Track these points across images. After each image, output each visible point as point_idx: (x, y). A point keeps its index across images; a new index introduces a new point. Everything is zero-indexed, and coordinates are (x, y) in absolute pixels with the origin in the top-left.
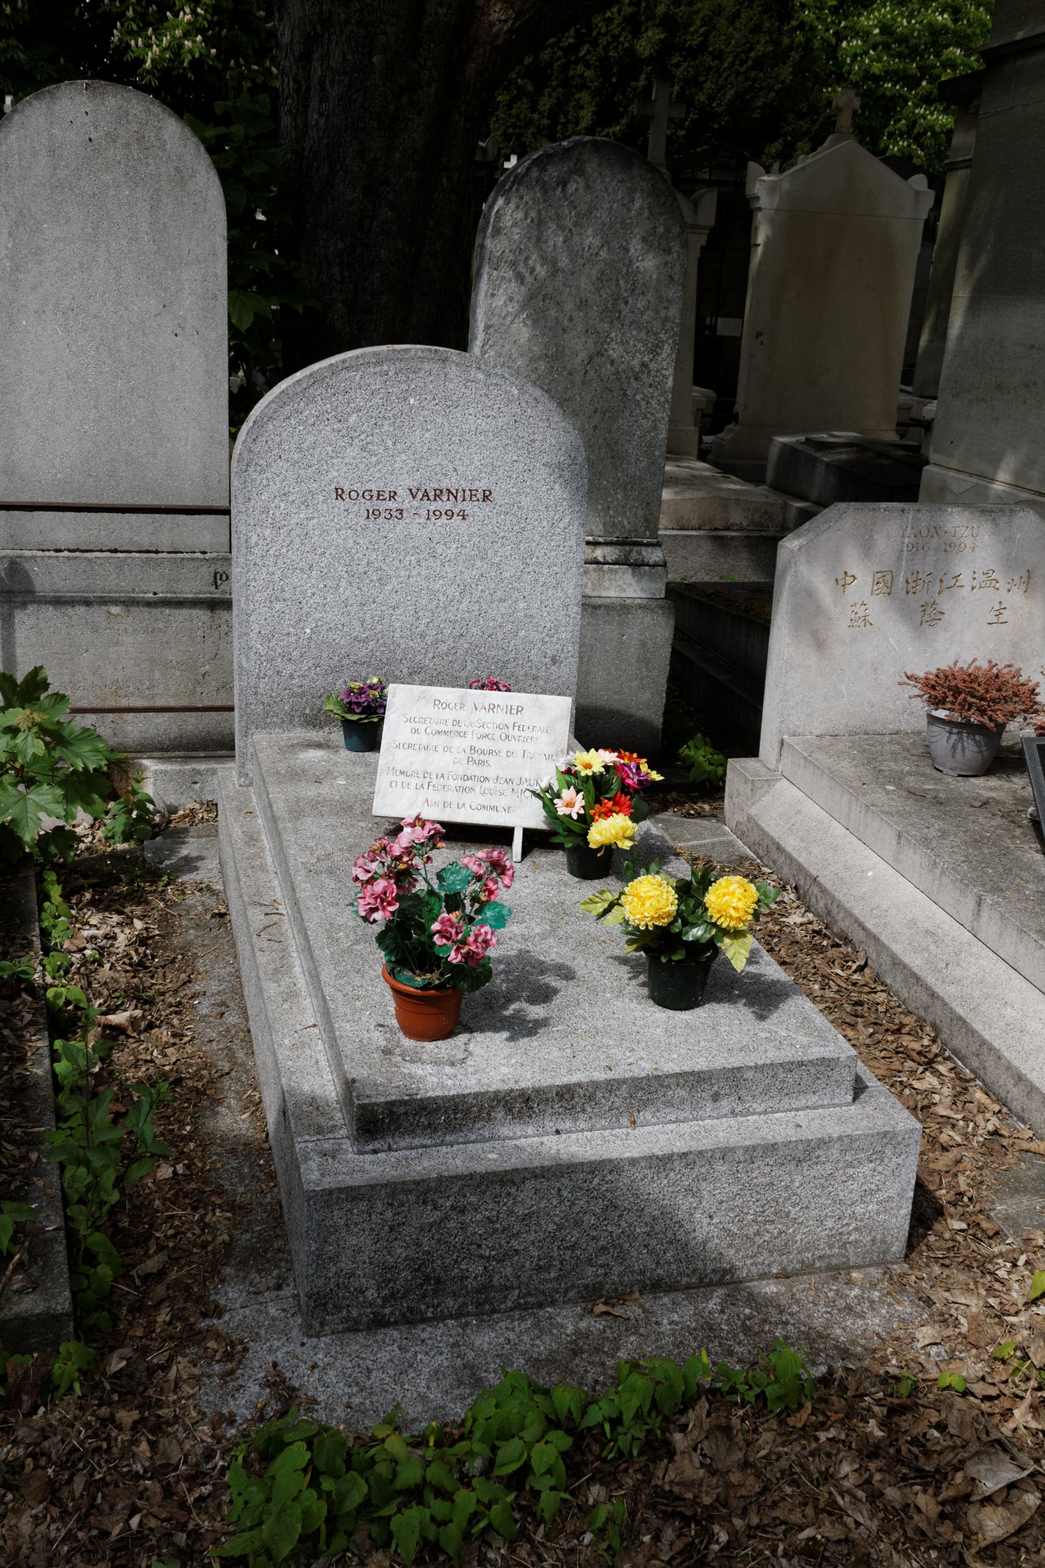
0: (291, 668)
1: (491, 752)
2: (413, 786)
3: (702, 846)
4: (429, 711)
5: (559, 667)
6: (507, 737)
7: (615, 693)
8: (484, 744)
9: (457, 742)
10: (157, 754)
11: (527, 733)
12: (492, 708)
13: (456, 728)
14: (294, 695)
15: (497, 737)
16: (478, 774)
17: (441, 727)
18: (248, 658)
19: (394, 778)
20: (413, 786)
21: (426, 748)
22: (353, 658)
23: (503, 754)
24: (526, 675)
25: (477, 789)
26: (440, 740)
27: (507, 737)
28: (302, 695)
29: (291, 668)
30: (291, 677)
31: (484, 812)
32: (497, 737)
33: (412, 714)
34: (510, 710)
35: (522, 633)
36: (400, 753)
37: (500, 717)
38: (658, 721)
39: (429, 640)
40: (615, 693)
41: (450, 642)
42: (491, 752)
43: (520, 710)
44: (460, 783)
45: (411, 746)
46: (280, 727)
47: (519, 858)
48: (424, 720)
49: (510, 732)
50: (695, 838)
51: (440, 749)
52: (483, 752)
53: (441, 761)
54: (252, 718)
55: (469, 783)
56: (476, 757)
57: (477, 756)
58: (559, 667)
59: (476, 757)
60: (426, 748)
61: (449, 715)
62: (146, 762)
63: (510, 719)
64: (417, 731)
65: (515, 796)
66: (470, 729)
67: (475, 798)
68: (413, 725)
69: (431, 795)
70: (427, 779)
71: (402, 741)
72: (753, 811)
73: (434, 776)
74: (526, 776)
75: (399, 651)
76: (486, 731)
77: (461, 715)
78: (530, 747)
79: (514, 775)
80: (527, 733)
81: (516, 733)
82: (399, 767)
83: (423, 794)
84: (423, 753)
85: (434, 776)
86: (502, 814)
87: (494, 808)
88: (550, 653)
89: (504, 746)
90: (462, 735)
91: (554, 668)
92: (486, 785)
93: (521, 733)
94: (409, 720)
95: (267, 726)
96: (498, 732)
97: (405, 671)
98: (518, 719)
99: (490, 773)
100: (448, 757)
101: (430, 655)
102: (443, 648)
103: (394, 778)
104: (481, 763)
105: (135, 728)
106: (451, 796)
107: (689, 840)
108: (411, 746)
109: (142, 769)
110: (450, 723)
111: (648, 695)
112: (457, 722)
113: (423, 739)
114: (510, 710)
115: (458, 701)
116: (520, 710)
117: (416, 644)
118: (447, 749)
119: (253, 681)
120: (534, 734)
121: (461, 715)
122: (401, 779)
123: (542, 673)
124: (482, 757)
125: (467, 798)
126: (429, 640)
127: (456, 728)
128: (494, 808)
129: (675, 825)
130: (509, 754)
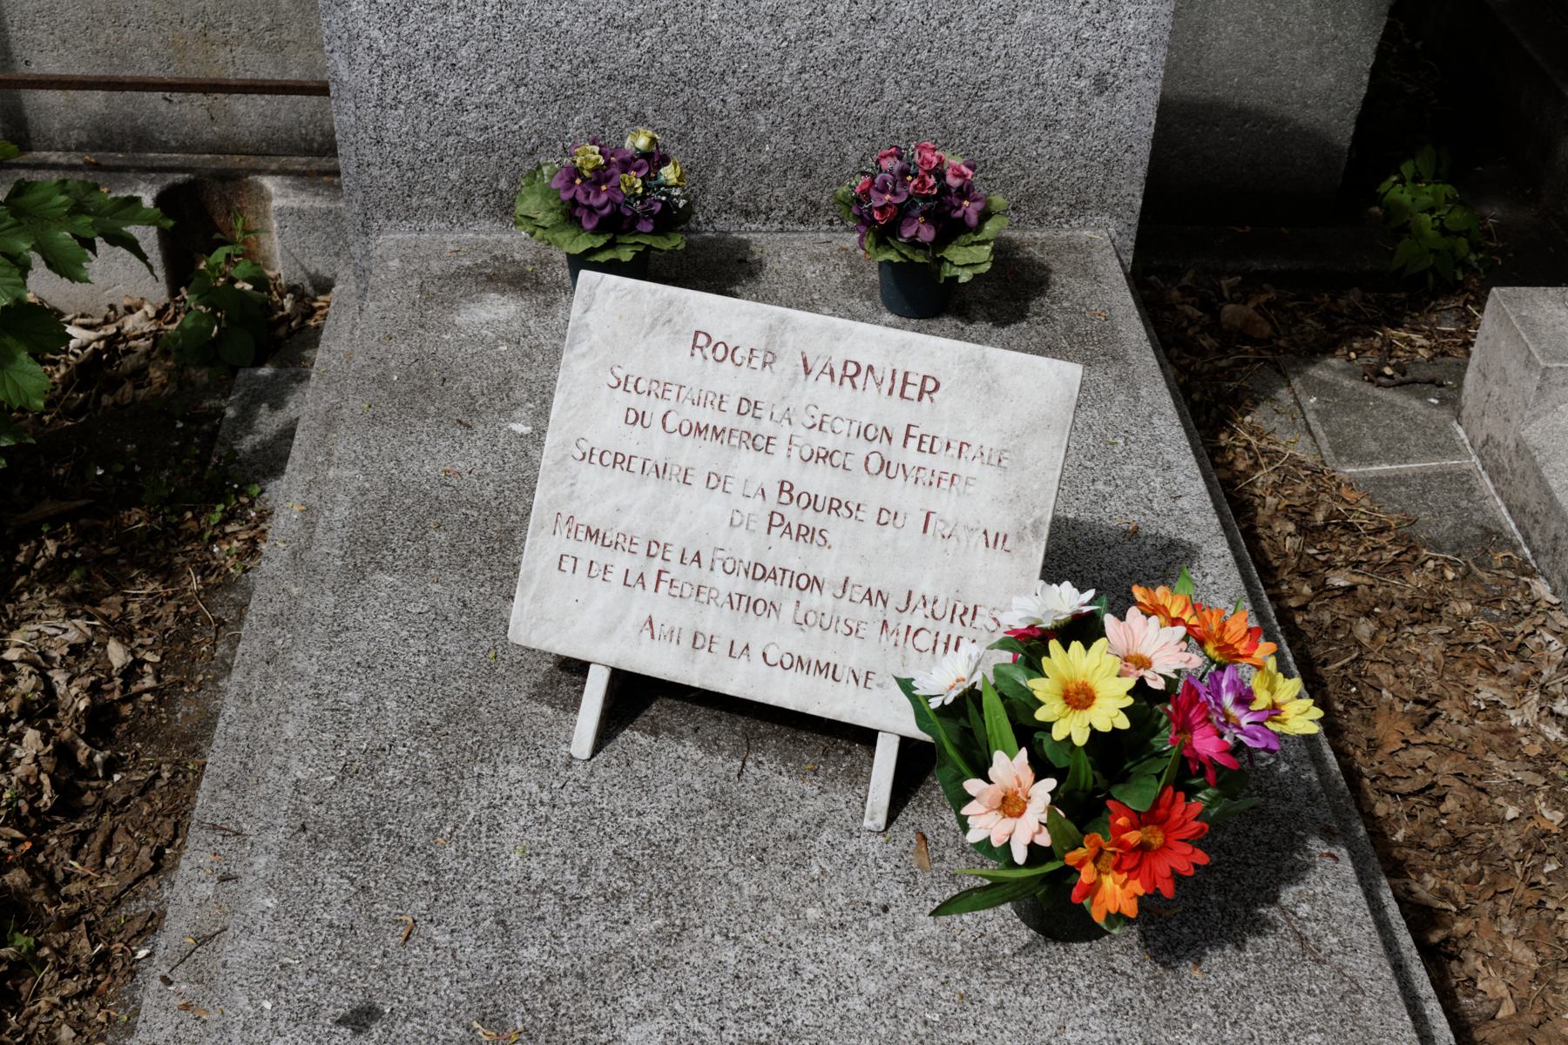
0: (455, 86)
1: (834, 506)
2: (616, 576)
3: (1400, 480)
4: (677, 362)
5: (1112, 102)
6: (885, 465)
7: (1259, 71)
8: (819, 480)
9: (747, 466)
10: (298, 162)
11: (942, 462)
12: (853, 373)
13: (747, 423)
14: (468, 147)
15: (855, 463)
16: (795, 565)
17: (707, 416)
18: (351, 62)
19: (570, 547)
20: (616, 576)
21: (661, 472)
22: (606, 67)
23: (869, 515)
24: (1028, 116)
25: (788, 609)
26: (698, 454)
27: (885, 465)
28: (488, 148)
29: (455, 86)
30: (459, 105)
31: (797, 678)
32: (855, 463)
33: (632, 367)
34: (900, 385)
35: (1026, 18)
36: (590, 474)
37: (872, 405)
38: (1343, 131)
39: (792, 28)
40: (1259, 71)
41: (845, 35)
42: (834, 506)
43: (929, 388)
44: (741, 584)
45: (621, 461)
46: (441, 217)
47: (881, 820)
48: (661, 389)
49: (895, 453)
50: (1387, 454)
51: (698, 480)
52: (812, 502)
53: (695, 516)
54: (375, 196)
55: (766, 589)
56: (793, 514)
57: (798, 514)
58: (1112, 102)
59: (793, 514)
60: (661, 472)
61: (730, 381)
62: (269, 183)
63: (897, 414)
64: (640, 418)
65: (887, 641)
66: (784, 432)
67: (777, 634)
68: (633, 400)
69: (662, 607)
70: (658, 563)
71: (599, 443)
72: (1533, 434)
73: (674, 556)
74: (925, 587)
75: (717, 55)
76: (828, 442)
77: (763, 384)
78: (944, 503)
79: (892, 580)
80: (942, 462)
81: (912, 457)
82: (586, 518)
83: (643, 603)
84: (652, 485)
85: (674, 556)
86: (847, 689)
87: (828, 670)
88: (1091, 67)
89: (873, 492)
90: (762, 444)
91: (1099, 102)
92: (813, 599)
93: (925, 459)
94: (622, 384)
95: (410, 213)
96: (861, 448)
97: (732, 99)
98: (922, 415)
99: (826, 565)
100: (718, 505)
101: (795, 65)
102: (827, 48)
103: (570, 547)
104: (806, 534)
105: (250, 114)
106: (716, 620)
107: (1371, 458)
108: (621, 461)
109: (263, 196)
110: (731, 405)
111: (1329, 77)
112: (748, 406)
113: (653, 444)
114: (900, 385)
115: (760, 343)
116: (929, 388)
117: (761, 39)
118: (717, 481)
119: (369, 112)
120: (962, 468)
121: (763, 384)
122: (588, 550)
123: (1069, 114)
124: (809, 517)
125: (759, 631)
126: (792, 28)
127: (747, 423)
128: (828, 670)
129: (1353, 404)
130: (886, 517)
